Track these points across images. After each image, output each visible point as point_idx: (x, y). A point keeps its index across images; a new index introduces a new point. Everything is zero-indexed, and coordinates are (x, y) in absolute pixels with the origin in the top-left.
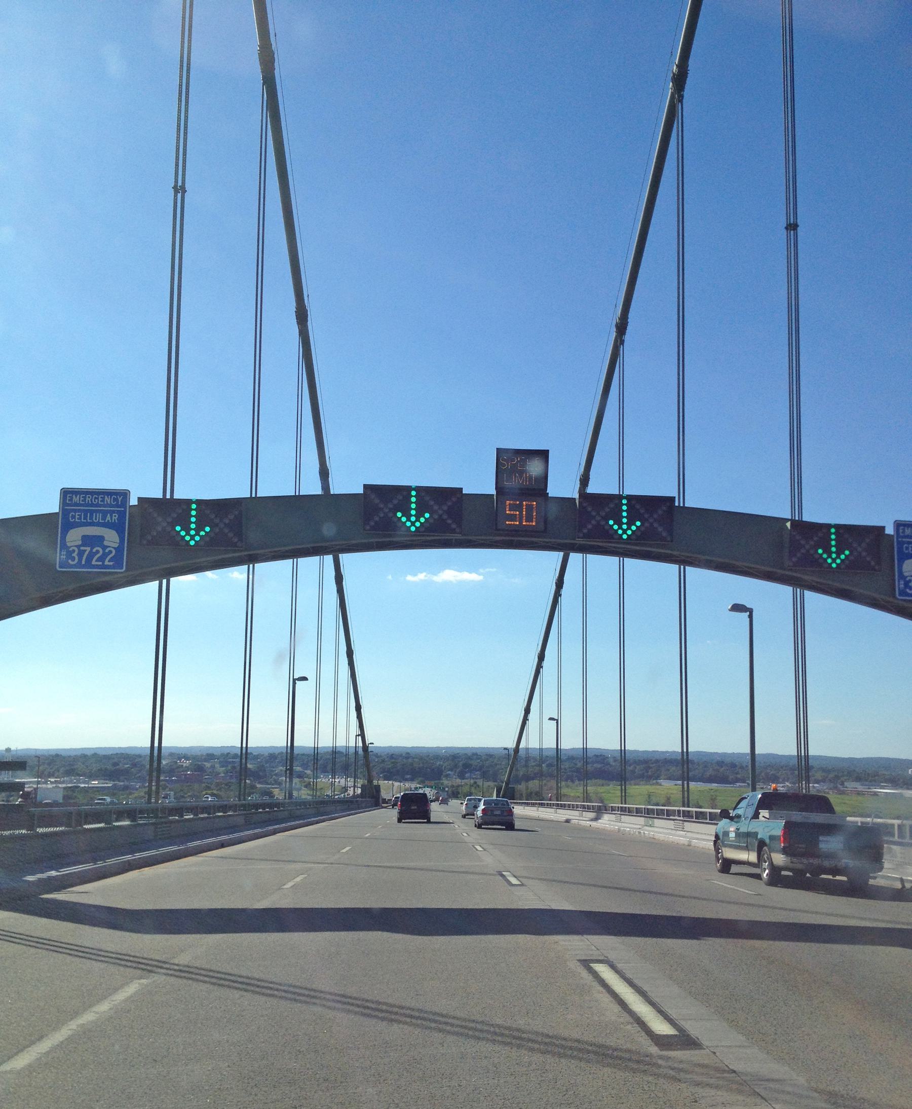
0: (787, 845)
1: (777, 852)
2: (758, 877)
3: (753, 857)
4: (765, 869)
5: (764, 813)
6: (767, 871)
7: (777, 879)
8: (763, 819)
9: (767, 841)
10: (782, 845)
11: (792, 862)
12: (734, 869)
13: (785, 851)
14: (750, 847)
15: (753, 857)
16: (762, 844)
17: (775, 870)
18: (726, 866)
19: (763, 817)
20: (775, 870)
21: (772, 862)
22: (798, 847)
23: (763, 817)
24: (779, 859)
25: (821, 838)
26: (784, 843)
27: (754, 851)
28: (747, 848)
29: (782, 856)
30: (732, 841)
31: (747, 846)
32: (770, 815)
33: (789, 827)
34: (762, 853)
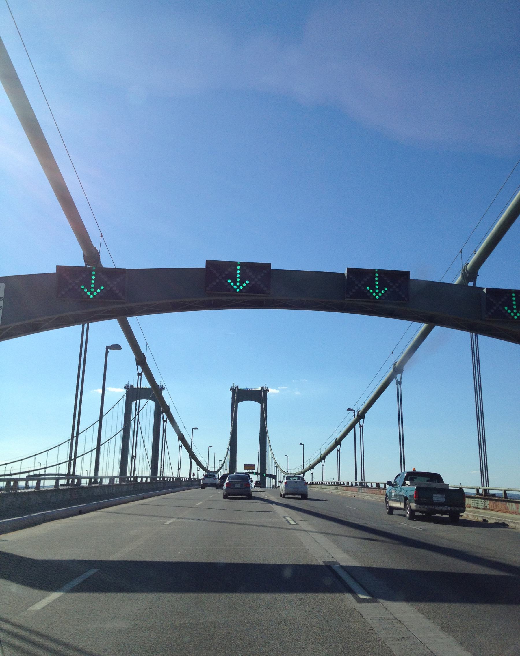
0: (417, 499)
1: (412, 503)
2: (405, 516)
3: (402, 505)
4: (408, 512)
5: (408, 483)
6: (409, 512)
7: (413, 516)
8: (407, 486)
9: (409, 497)
10: (415, 499)
11: (419, 508)
12: (395, 512)
13: (416, 502)
14: (401, 500)
15: (402, 505)
16: (406, 498)
17: (412, 512)
18: (391, 510)
19: (407, 485)
20: (412, 512)
21: (411, 507)
22: (423, 500)
23: (407, 485)
24: (413, 506)
25: (434, 495)
26: (416, 498)
27: (402, 502)
28: (399, 501)
29: (415, 504)
30: (394, 497)
31: (400, 500)
32: (410, 484)
33: (418, 490)
34: (406, 504)
